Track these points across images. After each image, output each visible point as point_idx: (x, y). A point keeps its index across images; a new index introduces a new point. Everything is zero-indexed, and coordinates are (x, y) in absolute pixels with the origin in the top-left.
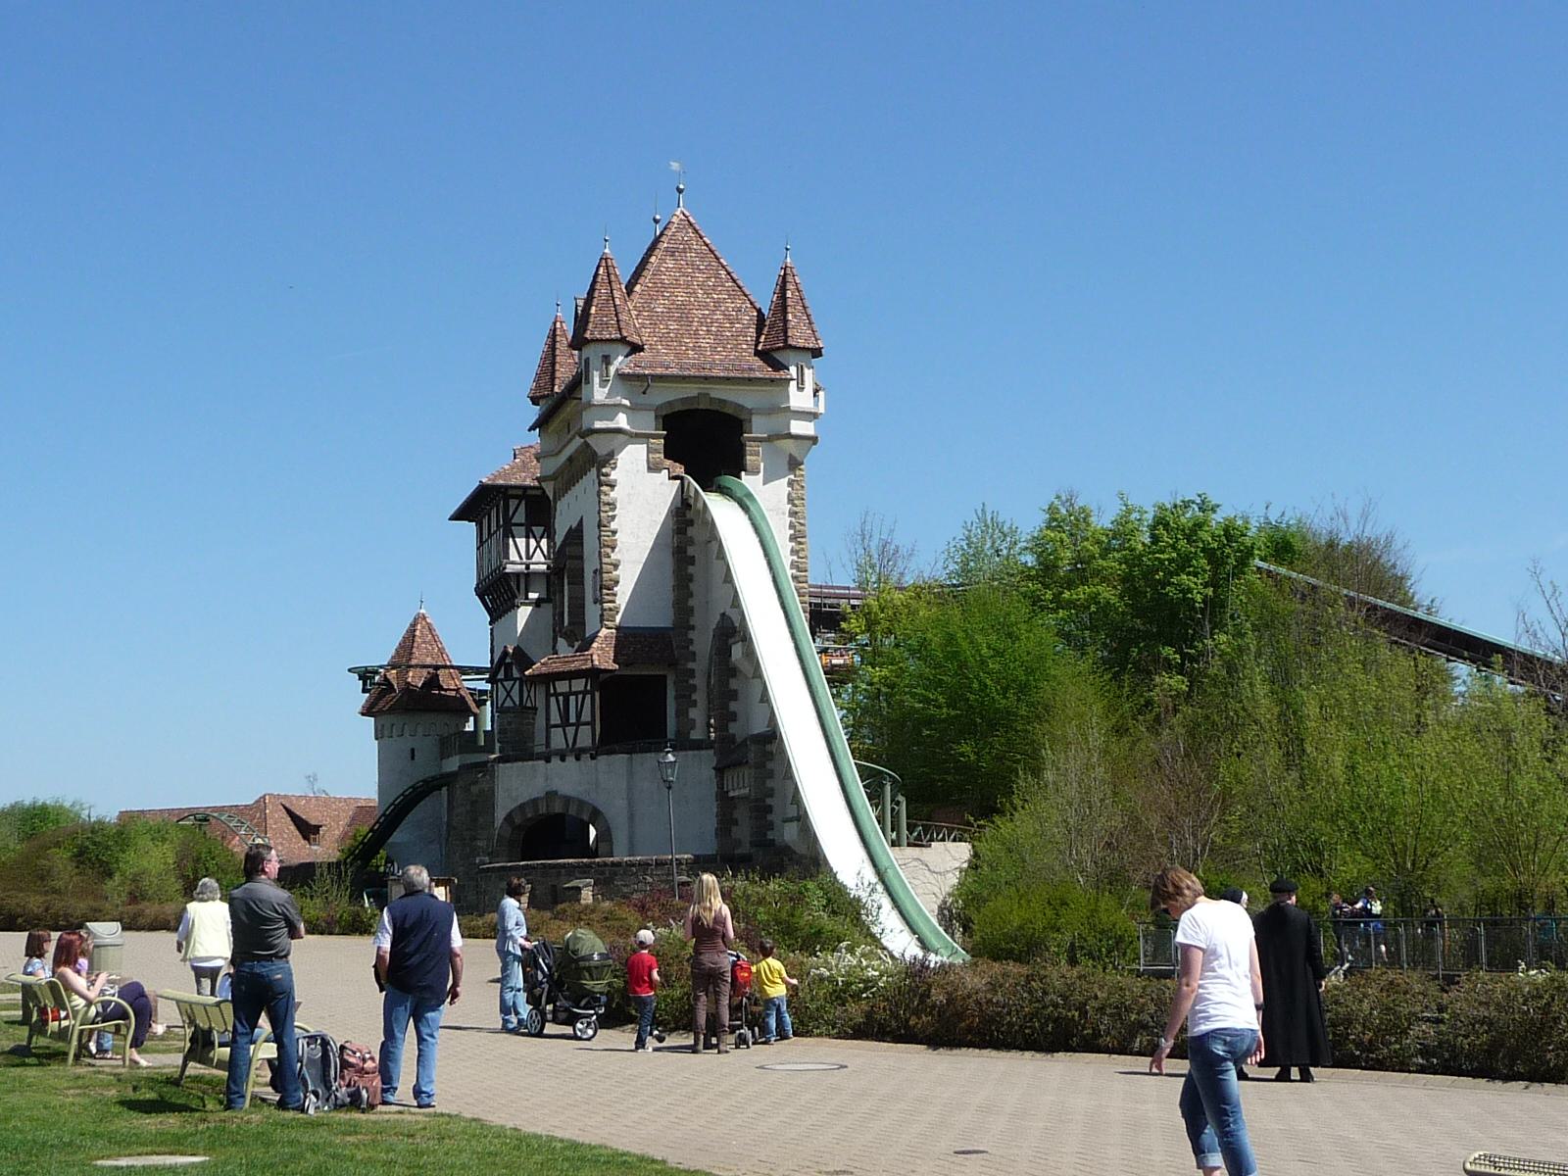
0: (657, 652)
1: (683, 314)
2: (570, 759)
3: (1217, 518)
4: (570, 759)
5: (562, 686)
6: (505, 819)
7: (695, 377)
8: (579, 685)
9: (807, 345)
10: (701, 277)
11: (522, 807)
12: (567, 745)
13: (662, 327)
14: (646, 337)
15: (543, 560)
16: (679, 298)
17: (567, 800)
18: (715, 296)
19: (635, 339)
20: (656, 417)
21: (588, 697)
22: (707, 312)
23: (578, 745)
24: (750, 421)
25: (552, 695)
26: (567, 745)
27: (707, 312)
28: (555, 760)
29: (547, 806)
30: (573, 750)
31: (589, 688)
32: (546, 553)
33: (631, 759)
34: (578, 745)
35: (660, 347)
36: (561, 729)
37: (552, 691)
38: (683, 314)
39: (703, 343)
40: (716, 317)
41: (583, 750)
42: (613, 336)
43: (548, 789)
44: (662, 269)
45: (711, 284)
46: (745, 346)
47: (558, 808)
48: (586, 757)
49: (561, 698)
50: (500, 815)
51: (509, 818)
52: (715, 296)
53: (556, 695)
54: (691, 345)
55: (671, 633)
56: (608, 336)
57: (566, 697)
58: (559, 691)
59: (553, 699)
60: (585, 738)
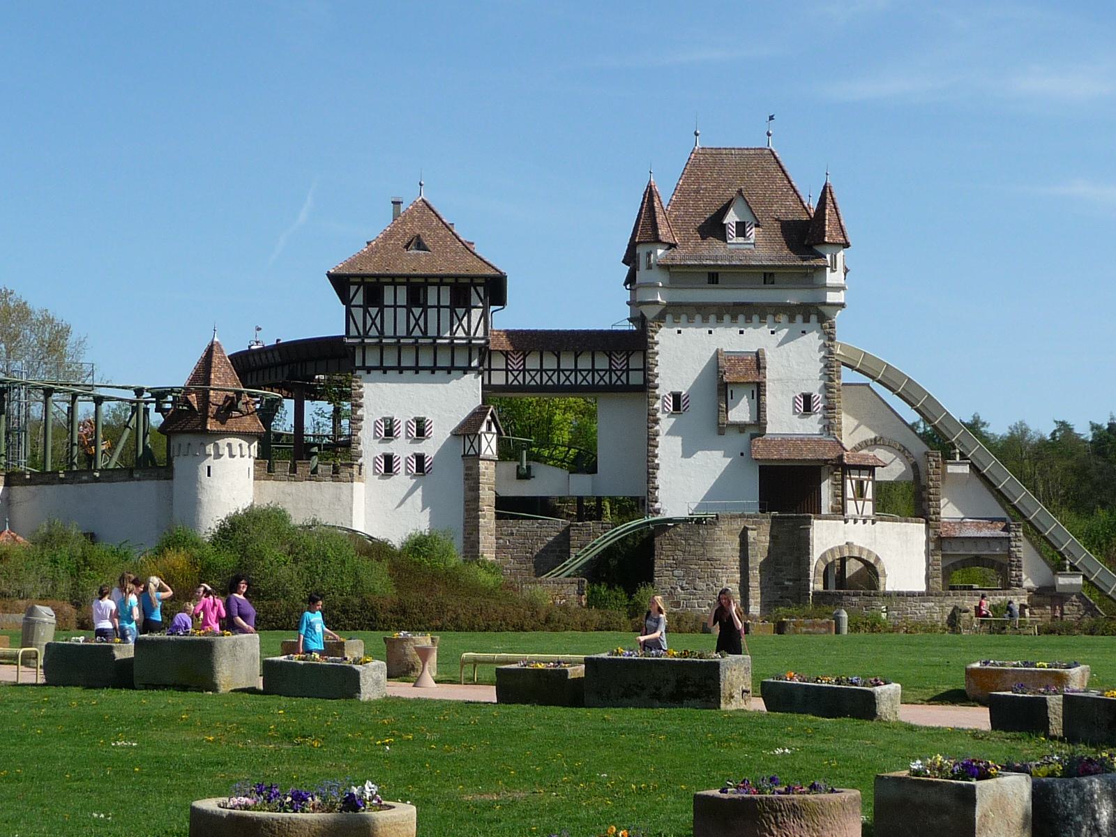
6: (820, 558)
11: (832, 550)
12: (858, 513)
15: (464, 335)
17: (861, 549)
23: (864, 514)
26: (858, 513)
32: (466, 330)
36: (866, 502)
48: (869, 522)
49: (854, 482)
50: (815, 555)
51: (823, 557)
53: (851, 479)
59: (849, 481)
60: (869, 508)
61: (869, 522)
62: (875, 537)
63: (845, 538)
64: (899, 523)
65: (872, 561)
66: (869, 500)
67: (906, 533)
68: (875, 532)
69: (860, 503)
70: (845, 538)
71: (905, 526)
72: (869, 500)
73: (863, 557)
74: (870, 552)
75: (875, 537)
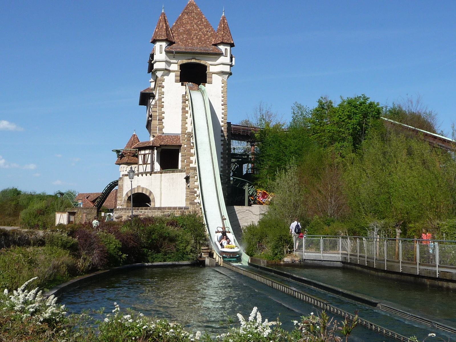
0: (175, 141)
1: (189, 32)
2: (144, 175)
3: (368, 102)
4: (144, 175)
5: (143, 152)
6: (126, 194)
7: (190, 52)
8: (147, 152)
9: (228, 42)
10: (196, 21)
13: (181, 36)
14: (175, 39)
16: (188, 27)
17: (143, 188)
18: (200, 27)
19: (171, 39)
20: (178, 66)
21: (150, 155)
22: (197, 32)
24: (209, 67)
25: (140, 155)
27: (197, 32)
28: (140, 175)
29: (137, 190)
30: (145, 172)
31: (150, 152)
33: (161, 176)
34: (146, 171)
35: (180, 43)
37: (140, 153)
38: (189, 32)
39: (194, 41)
40: (199, 33)
41: (148, 172)
42: (163, 38)
43: (138, 185)
44: (183, 18)
45: (199, 23)
46: (208, 43)
47: (140, 191)
48: (148, 175)
49: (142, 156)
51: (127, 194)
52: (200, 27)
54: (190, 42)
55: (180, 135)
56: (161, 39)
57: (144, 155)
58: (142, 153)
61: (148, 175)
62: (152, 182)
63: (138, 184)
64: (168, 174)
65: (148, 194)
66: (149, 164)
67: (173, 178)
68: (151, 179)
69: (145, 166)
70: (138, 184)
71: (172, 175)
72: (149, 164)
73: (143, 193)
74: (147, 190)
75: (152, 182)
